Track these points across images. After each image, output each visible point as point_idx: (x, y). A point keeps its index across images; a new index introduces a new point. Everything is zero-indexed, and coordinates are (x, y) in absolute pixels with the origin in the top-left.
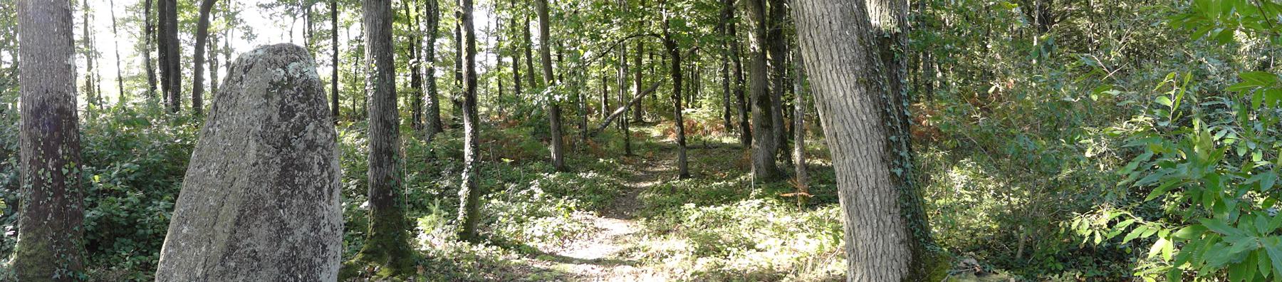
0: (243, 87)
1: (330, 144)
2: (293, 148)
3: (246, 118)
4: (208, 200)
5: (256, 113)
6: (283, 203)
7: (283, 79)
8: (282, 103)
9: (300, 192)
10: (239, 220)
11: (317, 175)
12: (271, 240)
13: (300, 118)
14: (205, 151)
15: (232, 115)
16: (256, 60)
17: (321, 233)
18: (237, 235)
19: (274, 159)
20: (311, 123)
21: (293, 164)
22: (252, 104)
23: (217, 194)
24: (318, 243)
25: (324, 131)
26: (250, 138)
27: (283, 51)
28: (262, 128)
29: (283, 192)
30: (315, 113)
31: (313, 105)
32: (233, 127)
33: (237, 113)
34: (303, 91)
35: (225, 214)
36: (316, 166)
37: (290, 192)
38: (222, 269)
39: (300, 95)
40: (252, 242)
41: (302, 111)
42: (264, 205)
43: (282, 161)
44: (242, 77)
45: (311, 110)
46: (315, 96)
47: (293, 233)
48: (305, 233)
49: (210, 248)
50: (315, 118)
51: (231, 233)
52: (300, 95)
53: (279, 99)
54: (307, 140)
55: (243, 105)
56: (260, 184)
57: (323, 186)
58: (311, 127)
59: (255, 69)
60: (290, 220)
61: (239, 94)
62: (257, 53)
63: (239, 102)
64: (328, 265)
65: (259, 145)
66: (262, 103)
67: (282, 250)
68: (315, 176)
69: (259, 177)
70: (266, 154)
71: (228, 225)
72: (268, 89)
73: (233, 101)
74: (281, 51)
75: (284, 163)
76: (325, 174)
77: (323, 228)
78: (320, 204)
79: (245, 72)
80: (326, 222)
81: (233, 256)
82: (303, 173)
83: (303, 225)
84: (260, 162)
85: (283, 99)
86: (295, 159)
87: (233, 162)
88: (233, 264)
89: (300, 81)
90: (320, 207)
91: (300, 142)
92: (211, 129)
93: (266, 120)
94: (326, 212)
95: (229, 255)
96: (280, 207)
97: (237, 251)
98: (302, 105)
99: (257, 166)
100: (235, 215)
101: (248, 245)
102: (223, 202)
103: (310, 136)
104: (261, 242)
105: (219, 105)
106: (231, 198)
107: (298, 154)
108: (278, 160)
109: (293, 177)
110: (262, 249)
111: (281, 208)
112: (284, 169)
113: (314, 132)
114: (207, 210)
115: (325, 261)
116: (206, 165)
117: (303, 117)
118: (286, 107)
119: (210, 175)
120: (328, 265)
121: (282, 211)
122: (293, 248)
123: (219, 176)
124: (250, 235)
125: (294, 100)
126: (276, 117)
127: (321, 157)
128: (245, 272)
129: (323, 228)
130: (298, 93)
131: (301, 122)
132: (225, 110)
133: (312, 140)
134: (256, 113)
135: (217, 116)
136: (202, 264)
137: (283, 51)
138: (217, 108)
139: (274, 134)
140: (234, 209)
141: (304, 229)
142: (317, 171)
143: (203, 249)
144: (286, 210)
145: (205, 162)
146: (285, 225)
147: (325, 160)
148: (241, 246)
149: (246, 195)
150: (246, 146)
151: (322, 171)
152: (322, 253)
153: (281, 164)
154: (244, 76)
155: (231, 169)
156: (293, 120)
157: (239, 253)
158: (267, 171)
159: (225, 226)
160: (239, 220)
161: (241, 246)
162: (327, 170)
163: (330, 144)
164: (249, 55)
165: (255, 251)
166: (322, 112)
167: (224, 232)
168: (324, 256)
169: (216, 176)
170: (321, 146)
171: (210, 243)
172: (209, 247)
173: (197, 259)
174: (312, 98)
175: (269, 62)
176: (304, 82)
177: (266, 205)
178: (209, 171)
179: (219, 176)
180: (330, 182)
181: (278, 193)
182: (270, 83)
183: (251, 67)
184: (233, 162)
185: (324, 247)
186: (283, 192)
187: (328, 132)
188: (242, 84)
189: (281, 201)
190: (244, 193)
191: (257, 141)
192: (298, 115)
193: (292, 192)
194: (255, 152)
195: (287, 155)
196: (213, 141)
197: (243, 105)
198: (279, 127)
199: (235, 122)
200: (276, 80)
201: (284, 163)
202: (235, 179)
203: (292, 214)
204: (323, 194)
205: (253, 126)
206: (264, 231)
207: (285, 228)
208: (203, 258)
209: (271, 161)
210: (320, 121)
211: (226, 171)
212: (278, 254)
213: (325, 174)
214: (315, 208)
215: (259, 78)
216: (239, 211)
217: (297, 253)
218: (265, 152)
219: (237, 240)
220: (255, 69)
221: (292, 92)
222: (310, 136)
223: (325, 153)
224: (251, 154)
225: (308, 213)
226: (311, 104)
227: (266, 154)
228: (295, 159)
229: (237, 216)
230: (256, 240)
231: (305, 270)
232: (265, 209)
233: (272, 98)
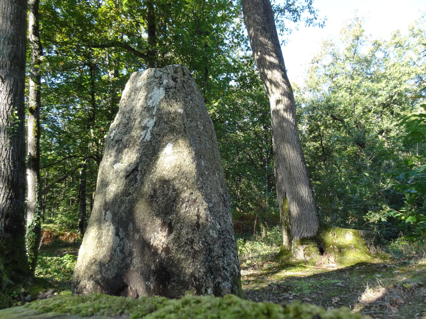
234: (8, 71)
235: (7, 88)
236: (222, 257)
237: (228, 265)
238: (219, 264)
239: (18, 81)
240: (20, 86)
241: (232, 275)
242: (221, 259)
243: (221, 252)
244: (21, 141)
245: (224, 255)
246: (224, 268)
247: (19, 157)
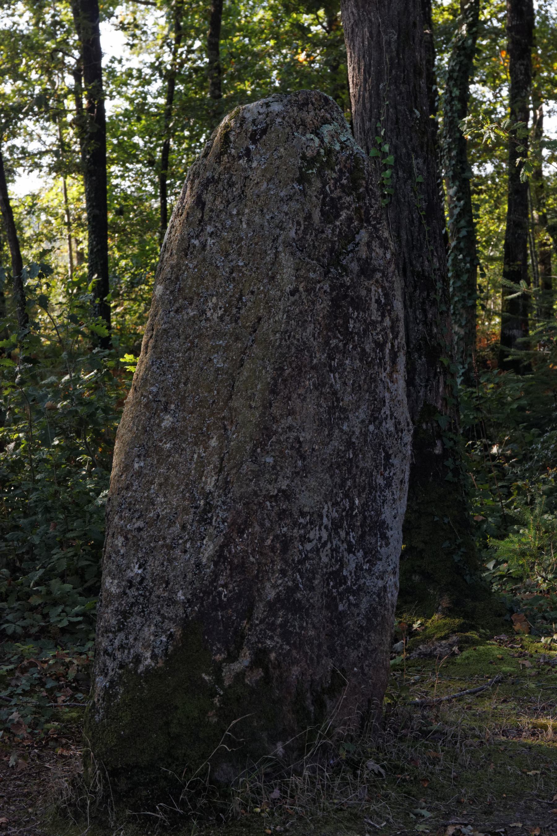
0: (254, 165)
2: (345, 269)
3: (268, 217)
4: (210, 360)
5: (285, 208)
7: (318, 153)
8: (322, 191)
9: (355, 348)
10: (275, 385)
12: (322, 423)
14: (189, 282)
15: (238, 214)
16: (273, 121)
18: (274, 410)
19: (322, 284)
20: (363, 231)
21: (346, 296)
22: (276, 195)
23: (227, 348)
26: (280, 249)
27: (310, 105)
28: (296, 233)
29: (333, 342)
30: (367, 212)
31: (364, 198)
32: (242, 234)
33: (247, 211)
34: (347, 174)
35: (249, 377)
36: (374, 306)
38: (255, 467)
40: (295, 425)
43: (332, 289)
44: (248, 150)
45: (361, 207)
46: (367, 183)
49: (227, 438)
50: (368, 221)
51: (265, 407)
52: (344, 181)
55: (258, 196)
56: (303, 324)
57: (385, 342)
58: (363, 236)
59: (273, 135)
61: (246, 178)
62: (270, 109)
63: (248, 192)
64: (393, 494)
65: (297, 261)
66: (292, 191)
69: (301, 312)
70: (311, 275)
71: (258, 395)
72: (300, 168)
73: (236, 190)
74: (308, 104)
75: (334, 293)
79: (254, 142)
81: (268, 448)
82: (359, 314)
83: (359, 407)
84: (301, 289)
85: (324, 187)
86: (348, 288)
87: (252, 292)
88: (270, 460)
89: (342, 157)
92: (196, 242)
93: (305, 219)
95: (263, 445)
97: (274, 439)
98: (348, 199)
99: (297, 296)
100: (268, 374)
101: (290, 428)
102: (242, 360)
103: (363, 253)
104: (307, 426)
105: (208, 198)
106: (256, 350)
107: (352, 279)
108: (327, 287)
109: (347, 318)
110: (308, 437)
112: (335, 303)
113: (368, 245)
114: (212, 378)
116: (195, 303)
118: (328, 199)
119: (207, 319)
120: (393, 494)
123: (227, 319)
124: (292, 412)
126: (317, 215)
127: (380, 290)
128: (289, 474)
130: (340, 178)
132: (221, 207)
134: (285, 208)
135: (206, 218)
136: (215, 467)
137: (310, 105)
138: (204, 204)
139: (316, 244)
140: (265, 368)
143: (214, 443)
145: (192, 298)
146: (338, 400)
147: (386, 295)
148: (280, 430)
149: (284, 343)
150: (273, 264)
154: (251, 147)
155: (249, 304)
156: (338, 223)
157: (279, 442)
158: (313, 303)
159: (251, 398)
160: (275, 385)
161: (280, 430)
162: (390, 314)
164: (256, 111)
167: (251, 407)
168: (386, 474)
169: (221, 318)
170: (379, 271)
171: (226, 430)
172: (224, 438)
173: (202, 464)
174: (361, 185)
175: (294, 122)
176: (348, 158)
178: (204, 312)
179: (227, 319)
181: (327, 343)
182: (302, 158)
183: (264, 131)
184: (252, 292)
185: (388, 457)
186: (333, 342)
187: (386, 248)
188: (250, 160)
189: (331, 358)
190: (281, 340)
191: (293, 254)
192: (344, 215)
193: (345, 345)
194: (293, 272)
196: (204, 260)
197: (258, 196)
198: (323, 232)
199: (245, 226)
200: (309, 153)
201: (334, 293)
202: (260, 319)
205: (282, 229)
206: (311, 408)
207: (337, 406)
208: (215, 458)
209: (318, 286)
210: (374, 227)
211: (240, 309)
212: (329, 450)
213: (387, 322)
214: (375, 381)
215: (282, 150)
216: (275, 369)
217: (354, 454)
218: (309, 271)
219: (275, 420)
220: (273, 135)
222: (363, 253)
224: (285, 276)
226: (360, 198)
227: (311, 275)
228: (348, 288)
229: (273, 378)
230: (299, 422)
231: (364, 491)
232: (312, 368)
233: (310, 183)
234: (354, 10)
235: (359, 64)
236: (114, 633)
237: (122, 647)
238: (101, 643)
239: (379, 32)
240: (389, 43)
241: (121, 667)
242: (110, 635)
243: (114, 622)
244: (406, 213)
245: (120, 630)
246: (106, 652)
247: (405, 263)
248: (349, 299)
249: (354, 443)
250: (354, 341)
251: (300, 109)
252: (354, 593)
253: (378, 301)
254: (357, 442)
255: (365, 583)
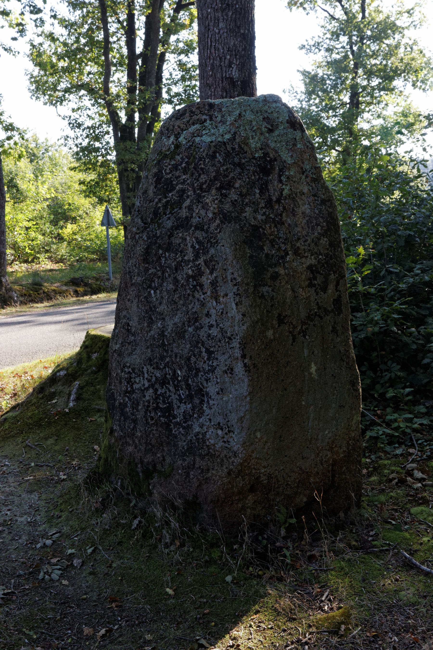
1: (213, 226)
6: (153, 285)
9: (169, 276)
11: (189, 261)
13: (178, 192)
17: (202, 333)
21: (156, 243)
24: (198, 342)
25: (203, 207)
37: (160, 273)
39: (184, 165)
41: (183, 183)
42: (132, 281)
43: (148, 238)
47: (164, 319)
48: (175, 324)
53: (155, 170)
54: (180, 218)
60: (160, 304)
67: (152, 332)
68: (185, 260)
75: (149, 241)
76: (201, 261)
77: (206, 329)
78: (197, 296)
80: (214, 323)
83: (176, 314)
85: (160, 171)
86: (158, 238)
90: (198, 300)
91: (169, 218)
94: (213, 312)
96: (150, 287)
98: (184, 177)
107: (161, 232)
111: (153, 289)
113: (190, 208)
115: (213, 370)
117: (183, 191)
121: (152, 292)
122: (162, 334)
125: (177, 170)
127: (194, 239)
129: (206, 329)
130: (182, 163)
131: (181, 196)
133: (187, 217)
141: (176, 320)
142: (190, 256)
144: (158, 291)
147: (199, 242)
151: (197, 256)
152: (209, 359)
153: (147, 241)
156: (170, 195)
163: (213, 226)
165: (128, 325)
166: (202, 184)
177: (134, 281)
180: (211, 273)
195: (152, 231)
201: (149, 241)
203: (162, 297)
204: (201, 286)
209: (137, 236)
221: (173, 162)
222: (184, 213)
223: (199, 234)
225: (181, 302)
228: (158, 238)
248: (157, 245)
249: (166, 336)
250: (167, 272)
251: (177, 119)
252: (184, 428)
253: (193, 247)
254: (168, 335)
255: (192, 425)
